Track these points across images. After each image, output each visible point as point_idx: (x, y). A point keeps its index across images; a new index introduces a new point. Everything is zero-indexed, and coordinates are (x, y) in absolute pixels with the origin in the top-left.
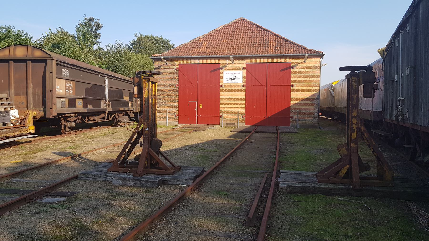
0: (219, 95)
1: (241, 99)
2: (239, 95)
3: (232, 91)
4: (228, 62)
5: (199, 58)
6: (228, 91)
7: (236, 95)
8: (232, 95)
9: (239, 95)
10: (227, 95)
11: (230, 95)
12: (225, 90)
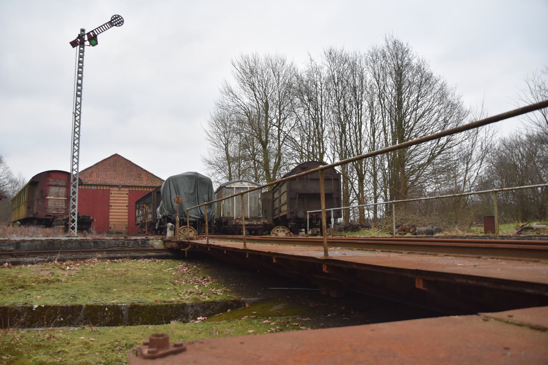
0: (109, 212)
1: (124, 215)
2: (123, 212)
3: (118, 209)
4: (115, 189)
5: (94, 185)
6: (115, 209)
7: (121, 212)
8: (119, 212)
9: (123, 212)
10: (114, 212)
11: (117, 212)
12: (114, 209)
